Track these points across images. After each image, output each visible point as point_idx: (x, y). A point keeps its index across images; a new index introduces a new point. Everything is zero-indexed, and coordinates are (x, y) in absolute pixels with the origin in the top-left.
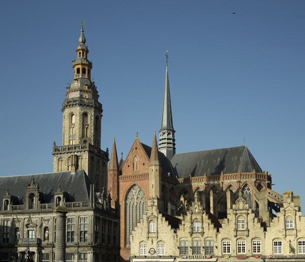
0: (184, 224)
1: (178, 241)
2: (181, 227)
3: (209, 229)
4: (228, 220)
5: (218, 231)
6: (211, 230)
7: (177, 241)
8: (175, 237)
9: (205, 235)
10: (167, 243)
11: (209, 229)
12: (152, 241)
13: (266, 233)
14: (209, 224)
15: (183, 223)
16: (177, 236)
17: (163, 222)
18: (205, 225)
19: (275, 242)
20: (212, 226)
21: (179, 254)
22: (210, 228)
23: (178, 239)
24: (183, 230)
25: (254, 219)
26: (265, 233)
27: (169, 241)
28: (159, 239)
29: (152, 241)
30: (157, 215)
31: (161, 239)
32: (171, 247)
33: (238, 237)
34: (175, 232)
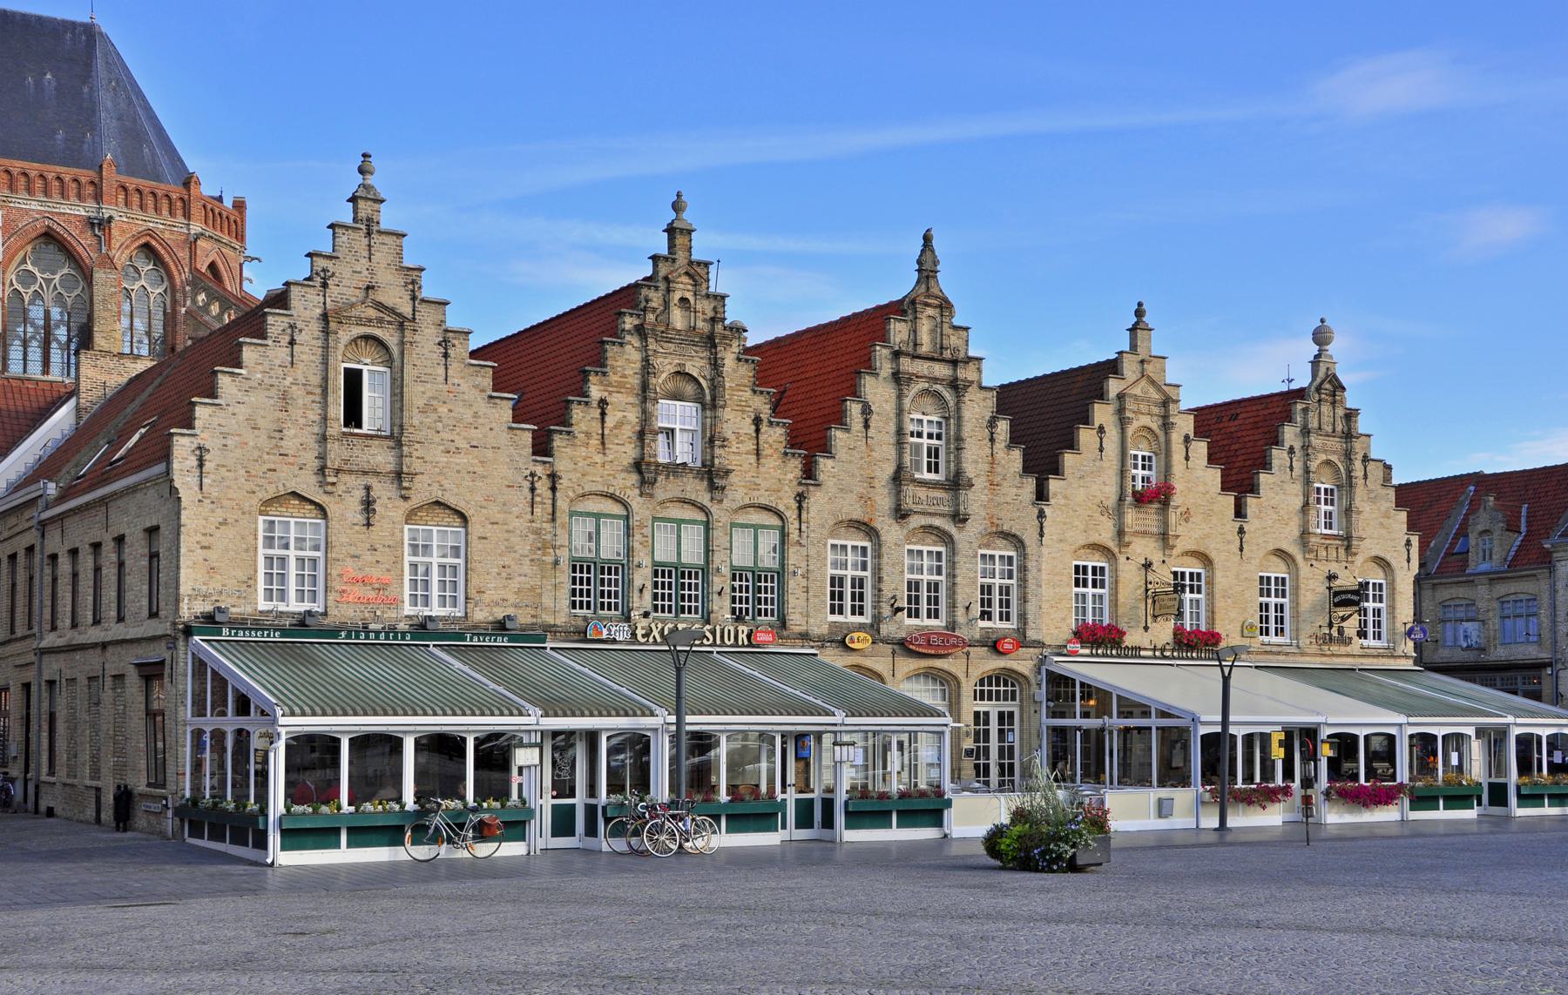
0: (603, 403)
1: (562, 517)
2: (582, 418)
3: (758, 453)
4: (867, 410)
5: (809, 472)
6: (772, 462)
7: (553, 520)
8: (543, 487)
9: (737, 492)
10: (476, 528)
11: (758, 453)
12: (368, 505)
13: (1047, 511)
14: (757, 421)
15: (595, 392)
16: (553, 477)
17: (454, 367)
18: (735, 422)
19: (1077, 567)
20: (775, 436)
21: (565, 602)
22: (766, 451)
23: (562, 504)
24: (595, 442)
25: (992, 423)
26: (1041, 515)
27: (494, 511)
28: (422, 491)
29: (368, 505)
30: (406, 309)
31: (437, 494)
32: (507, 560)
33: (916, 521)
34: (542, 447)
